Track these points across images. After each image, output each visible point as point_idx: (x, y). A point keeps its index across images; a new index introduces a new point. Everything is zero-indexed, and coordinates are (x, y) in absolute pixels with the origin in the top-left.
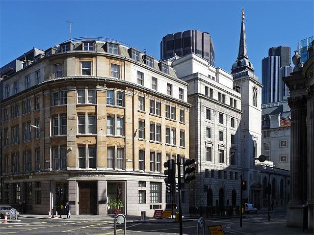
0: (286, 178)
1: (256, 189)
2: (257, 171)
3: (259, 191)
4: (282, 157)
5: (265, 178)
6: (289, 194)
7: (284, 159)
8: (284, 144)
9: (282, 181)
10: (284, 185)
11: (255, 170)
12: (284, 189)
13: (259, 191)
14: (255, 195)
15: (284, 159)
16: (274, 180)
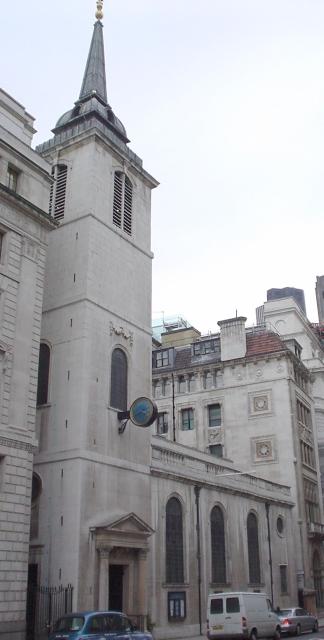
0: (267, 506)
1: (115, 542)
2: (133, 466)
3: (136, 553)
4: (260, 445)
5: (174, 505)
6: (283, 568)
7: (264, 450)
8: (261, 404)
9: (252, 518)
10: (263, 532)
11: (120, 462)
12: (264, 546)
13: (136, 553)
14: (117, 575)
15: (264, 450)
16: (218, 513)
